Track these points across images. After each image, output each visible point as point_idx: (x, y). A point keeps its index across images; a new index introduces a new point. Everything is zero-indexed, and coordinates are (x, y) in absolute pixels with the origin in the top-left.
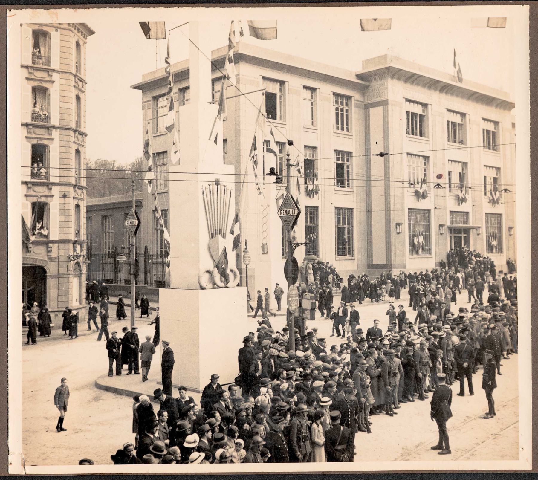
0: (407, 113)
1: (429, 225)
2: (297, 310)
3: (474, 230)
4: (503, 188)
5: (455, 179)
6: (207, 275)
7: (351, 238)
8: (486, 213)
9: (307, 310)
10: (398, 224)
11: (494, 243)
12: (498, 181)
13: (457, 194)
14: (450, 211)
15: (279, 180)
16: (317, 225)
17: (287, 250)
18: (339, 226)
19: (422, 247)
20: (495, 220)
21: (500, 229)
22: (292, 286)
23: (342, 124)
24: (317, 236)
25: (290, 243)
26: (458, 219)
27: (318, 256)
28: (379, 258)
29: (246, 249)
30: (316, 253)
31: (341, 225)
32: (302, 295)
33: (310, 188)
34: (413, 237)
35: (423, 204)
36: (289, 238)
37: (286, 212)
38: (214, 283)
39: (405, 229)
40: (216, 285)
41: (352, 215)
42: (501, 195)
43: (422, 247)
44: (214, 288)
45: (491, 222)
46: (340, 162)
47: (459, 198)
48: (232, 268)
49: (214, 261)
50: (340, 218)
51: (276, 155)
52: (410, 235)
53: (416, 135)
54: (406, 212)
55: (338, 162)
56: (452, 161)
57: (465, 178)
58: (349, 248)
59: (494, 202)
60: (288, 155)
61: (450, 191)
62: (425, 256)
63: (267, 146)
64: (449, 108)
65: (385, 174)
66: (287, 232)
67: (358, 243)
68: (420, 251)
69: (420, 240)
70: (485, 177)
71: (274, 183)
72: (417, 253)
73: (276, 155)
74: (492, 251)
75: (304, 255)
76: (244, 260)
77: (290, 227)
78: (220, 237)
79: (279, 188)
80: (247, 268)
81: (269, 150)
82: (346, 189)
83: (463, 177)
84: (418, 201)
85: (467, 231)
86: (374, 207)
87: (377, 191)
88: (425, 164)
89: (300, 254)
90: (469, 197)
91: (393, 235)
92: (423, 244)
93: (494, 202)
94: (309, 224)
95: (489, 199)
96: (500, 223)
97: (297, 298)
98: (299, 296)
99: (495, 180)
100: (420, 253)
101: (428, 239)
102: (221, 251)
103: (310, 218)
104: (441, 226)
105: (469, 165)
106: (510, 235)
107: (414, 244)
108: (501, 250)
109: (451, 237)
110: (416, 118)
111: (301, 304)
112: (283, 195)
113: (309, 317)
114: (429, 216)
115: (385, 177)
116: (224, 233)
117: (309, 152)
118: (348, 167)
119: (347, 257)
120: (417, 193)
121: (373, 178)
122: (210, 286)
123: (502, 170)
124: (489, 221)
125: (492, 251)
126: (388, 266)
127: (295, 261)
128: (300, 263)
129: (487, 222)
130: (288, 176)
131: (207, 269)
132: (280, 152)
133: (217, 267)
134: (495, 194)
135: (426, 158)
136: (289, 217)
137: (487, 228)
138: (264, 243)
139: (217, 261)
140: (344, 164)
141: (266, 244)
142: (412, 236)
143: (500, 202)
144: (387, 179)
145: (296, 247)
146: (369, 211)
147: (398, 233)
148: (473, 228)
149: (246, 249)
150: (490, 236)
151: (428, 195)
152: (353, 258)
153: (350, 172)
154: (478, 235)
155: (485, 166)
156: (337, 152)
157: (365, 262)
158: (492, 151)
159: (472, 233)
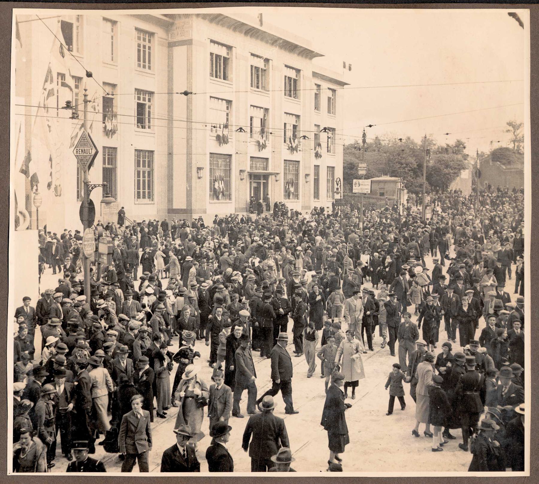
0: (212, 54)
1: (230, 170)
2: (93, 254)
3: (273, 176)
4: (302, 134)
5: (257, 124)
8: (285, 160)
9: (103, 254)
11: (292, 189)
12: (298, 129)
14: (251, 157)
15: (76, 115)
19: (223, 192)
20: (293, 167)
21: (297, 175)
22: (87, 230)
23: (144, 62)
26: (258, 166)
28: (179, 203)
32: (99, 238)
33: (109, 127)
35: (224, 149)
37: (82, 151)
39: (206, 174)
43: (223, 192)
45: (289, 169)
46: (141, 101)
50: (140, 161)
51: (71, 90)
53: (220, 78)
54: (208, 156)
55: (139, 102)
56: (254, 106)
59: (292, 149)
60: (86, 90)
61: (251, 137)
62: (225, 201)
63: (62, 80)
64: (253, 52)
66: (82, 172)
67: (159, 188)
68: (220, 196)
69: (220, 185)
71: (70, 118)
72: (218, 198)
73: (71, 90)
74: (289, 198)
75: (101, 198)
76: (34, 202)
77: (87, 167)
79: (74, 126)
80: (37, 210)
81: (64, 85)
82: (147, 130)
83: (264, 123)
85: (266, 177)
86: (175, 151)
87: (179, 134)
88: (228, 108)
89: (96, 196)
90: (269, 144)
93: (292, 149)
95: (289, 146)
96: (297, 170)
97: (94, 242)
98: (96, 240)
99: (295, 127)
100: (220, 198)
101: (228, 184)
104: (241, 171)
105: (270, 111)
106: (307, 182)
107: (215, 188)
108: (297, 196)
110: (220, 60)
111: (97, 248)
114: (230, 162)
117: (108, 89)
118: (149, 107)
120: (218, 138)
123: (301, 118)
124: (287, 168)
125: (289, 198)
126: (188, 211)
127: (91, 203)
129: (285, 169)
130: (85, 112)
132: (77, 87)
134: (294, 141)
135: (229, 102)
136: (86, 156)
137: (285, 174)
140: (145, 104)
141: (60, 186)
142: (213, 181)
143: (299, 149)
144: (189, 120)
145: (92, 188)
147: (199, 178)
148: (271, 174)
151: (229, 140)
152: (153, 202)
153: (151, 112)
154: (277, 181)
155: (285, 113)
156: (138, 91)
157: (164, 206)
158: (293, 98)
159: (271, 179)
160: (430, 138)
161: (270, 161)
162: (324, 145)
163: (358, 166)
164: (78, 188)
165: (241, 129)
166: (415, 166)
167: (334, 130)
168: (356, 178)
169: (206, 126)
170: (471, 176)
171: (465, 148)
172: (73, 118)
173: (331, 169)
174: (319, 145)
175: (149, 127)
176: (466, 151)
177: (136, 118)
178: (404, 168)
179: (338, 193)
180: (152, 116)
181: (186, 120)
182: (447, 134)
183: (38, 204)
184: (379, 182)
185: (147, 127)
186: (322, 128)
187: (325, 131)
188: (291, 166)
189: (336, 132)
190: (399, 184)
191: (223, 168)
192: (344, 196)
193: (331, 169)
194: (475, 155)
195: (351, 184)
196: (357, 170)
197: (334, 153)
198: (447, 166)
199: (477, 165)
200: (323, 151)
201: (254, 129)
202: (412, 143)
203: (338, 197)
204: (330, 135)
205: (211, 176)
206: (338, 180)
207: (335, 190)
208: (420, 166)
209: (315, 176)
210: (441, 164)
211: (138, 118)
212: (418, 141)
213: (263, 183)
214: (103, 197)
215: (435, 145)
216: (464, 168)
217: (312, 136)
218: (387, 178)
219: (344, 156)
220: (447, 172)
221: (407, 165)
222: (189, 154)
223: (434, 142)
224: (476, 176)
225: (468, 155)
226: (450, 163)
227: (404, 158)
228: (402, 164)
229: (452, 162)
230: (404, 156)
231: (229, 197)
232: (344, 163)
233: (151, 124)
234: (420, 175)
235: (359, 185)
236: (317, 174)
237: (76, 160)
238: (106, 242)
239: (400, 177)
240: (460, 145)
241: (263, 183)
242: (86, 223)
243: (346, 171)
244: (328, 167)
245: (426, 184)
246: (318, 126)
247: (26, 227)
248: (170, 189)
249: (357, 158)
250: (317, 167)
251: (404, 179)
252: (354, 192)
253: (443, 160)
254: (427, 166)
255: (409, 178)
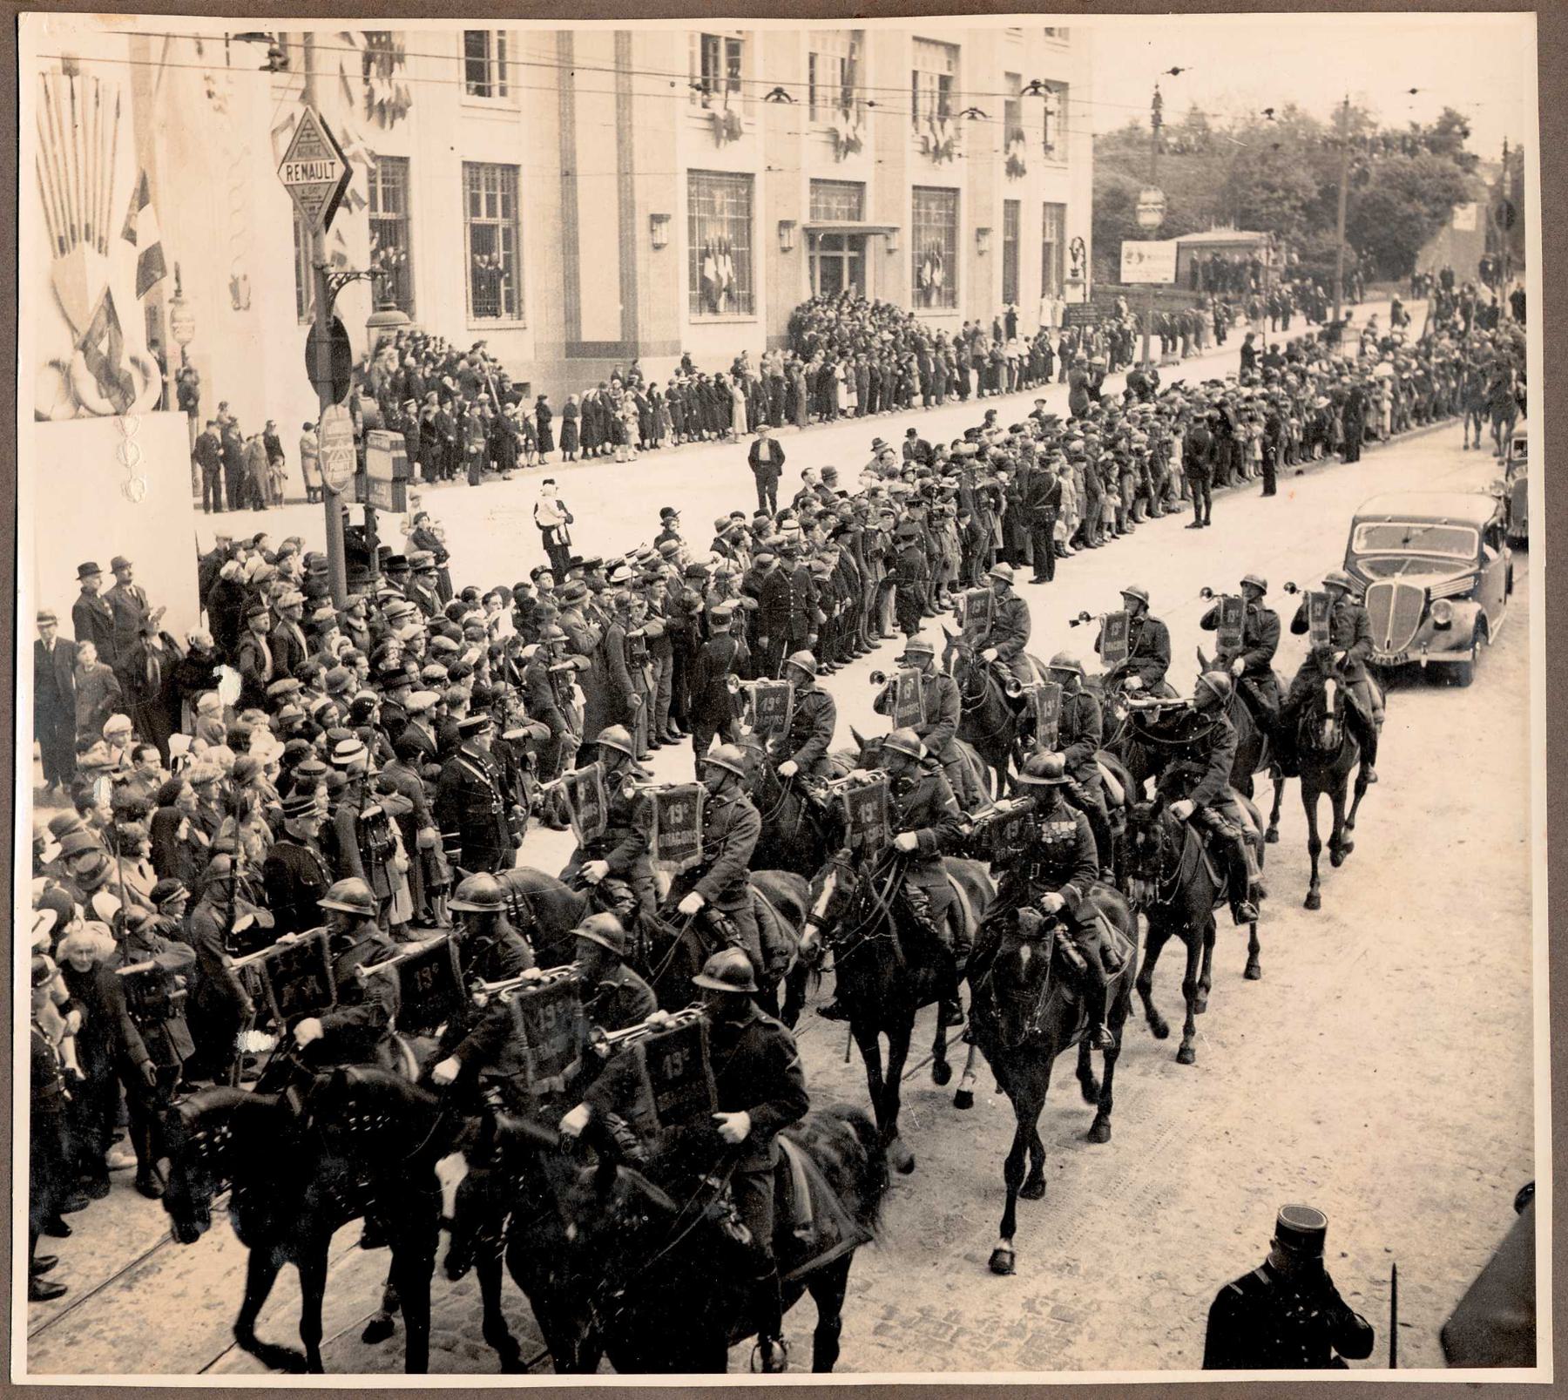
1: (749, 221)
2: (352, 484)
4: (966, 103)
6: (54, 376)
7: (514, 261)
8: (915, 188)
9: (379, 481)
10: (657, 219)
12: (953, 88)
13: (832, 125)
14: (814, 181)
15: (278, 60)
16: (408, 219)
17: (313, 298)
18: (476, 220)
19: (728, 290)
20: (939, 207)
21: (952, 234)
22: (331, 410)
24: (406, 252)
25: (321, 271)
26: (834, 206)
27: (411, 316)
28: (600, 325)
29: (178, 292)
30: (406, 305)
31: (483, 219)
32: (365, 434)
33: (383, 92)
34: (702, 260)
35: (729, 158)
36: (318, 256)
37: (304, 171)
38: (78, 402)
39: (676, 234)
40: (87, 408)
41: (516, 187)
42: (958, 129)
43: (728, 290)
44: (76, 416)
45: (928, 214)
47: (837, 136)
48: (134, 354)
49: (74, 329)
52: (692, 254)
54: (683, 178)
57: (858, 75)
58: (509, 294)
59: (939, 153)
61: (812, 117)
62: (736, 318)
65: (617, 56)
66: (310, 237)
69: (720, 269)
70: (915, 73)
71: (263, 68)
74: (928, 304)
75: (367, 312)
77: (320, 220)
78: (87, 249)
79: (279, 94)
80: (183, 353)
82: (495, 100)
83: (852, 71)
84: (718, 145)
85: (858, 241)
86: (582, 166)
91: (642, 253)
92: (730, 279)
94: (382, 215)
96: (953, 218)
97: (351, 445)
98: (357, 439)
99: (945, 82)
101: (743, 264)
102: (95, 299)
103: (384, 197)
104: (785, 225)
106: (981, 253)
107: (705, 280)
108: (951, 299)
109: (811, 258)
111: (361, 464)
112: (292, 117)
113: (388, 502)
114: (749, 195)
115: (617, 62)
116: (101, 239)
119: (505, 319)
121: (579, 61)
122: (67, 408)
123: (963, 52)
124: (923, 211)
125: (928, 304)
126: (626, 349)
127: (338, 330)
128: (360, 343)
129: (916, 215)
131: (54, 357)
133: (84, 348)
136: (315, 188)
137: (916, 230)
138: (239, 274)
139: (84, 328)
141: (245, 278)
143: (956, 151)
145: (340, 284)
146: (567, 174)
147: (657, 247)
148: (875, 232)
149: (178, 292)
150: (926, 258)
152: (520, 324)
154: (890, 252)
155: (916, 39)
157: (557, 336)
159: (873, 246)
160: (1360, 105)
161: (870, 191)
162: (1033, 134)
163: (1137, 199)
164: (298, 284)
165: (779, 91)
166: (1314, 195)
167: (1063, 87)
168: (1134, 238)
169: (673, 85)
170: (1483, 222)
171: (1466, 134)
172: (271, 68)
173: (1056, 211)
174: (1019, 136)
175: (503, 92)
176: (1469, 146)
177: (463, 63)
178: (1279, 202)
179: (1075, 284)
180: (509, 57)
181: (612, 66)
182: (1413, 91)
183: (184, 336)
184: (1202, 247)
185: (495, 91)
186: (1026, 83)
187: (1036, 93)
188: (933, 205)
189: (1072, 94)
190: (1264, 252)
191: (727, 215)
192: (1093, 293)
193: (1056, 211)
194: (1499, 158)
195: (1116, 257)
196: (1134, 212)
197: (1065, 160)
198: (1412, 194)
199: (1502, 188)
200: (1028, 153)
201: (819, 91)
202: (1304, 121)
203: (1075, 295)
204: (1053, 104)
205: (691, 241)
206: (1077, 245)
207: (1068, 276)
208: (1329, 194)
209: (1006, 232)
210: (1392, 187)
211: (468, 63)
212: (1323, 117)
213: (851, 259)
214: (375, 310)
215: (1374, 125)
216: (1463, 199)
217: (996, 109)
218: (1228, 234)
219: (1096, 170)
220: (1410, 210)
221: (1289, 190)
222: (625, 174)
223: (1372, 118)
224: (1500, 224)
225: (1475, 157)
226: (1421, 182)
227: (1279, 169)
228: (1273, 190)
229: (1428, 181)
230: (1279, 163)
231: (749, 304)
232: (1095, 191)
233: (509, 82)
234: (1327, 219)
235: (1141, 257)
236: (1012, 225)
237: (288, 201)
238: (387, 445)
239: (1267, 229)
240: (1452, 125)
241: (851, 259)
242: (328, 388)
243: (1102, 216)
244: (1046, 205)
245: (1348, 254)
246: (1014, 77)
247: (154, 404)
248: (571, 281)
249: (1134, 174)
250: (1012, 206)
251: (1278, 237)
252: (1123, 280)
253: (1399, 175)
254: (1350, 195)
255: (1294, 231)
